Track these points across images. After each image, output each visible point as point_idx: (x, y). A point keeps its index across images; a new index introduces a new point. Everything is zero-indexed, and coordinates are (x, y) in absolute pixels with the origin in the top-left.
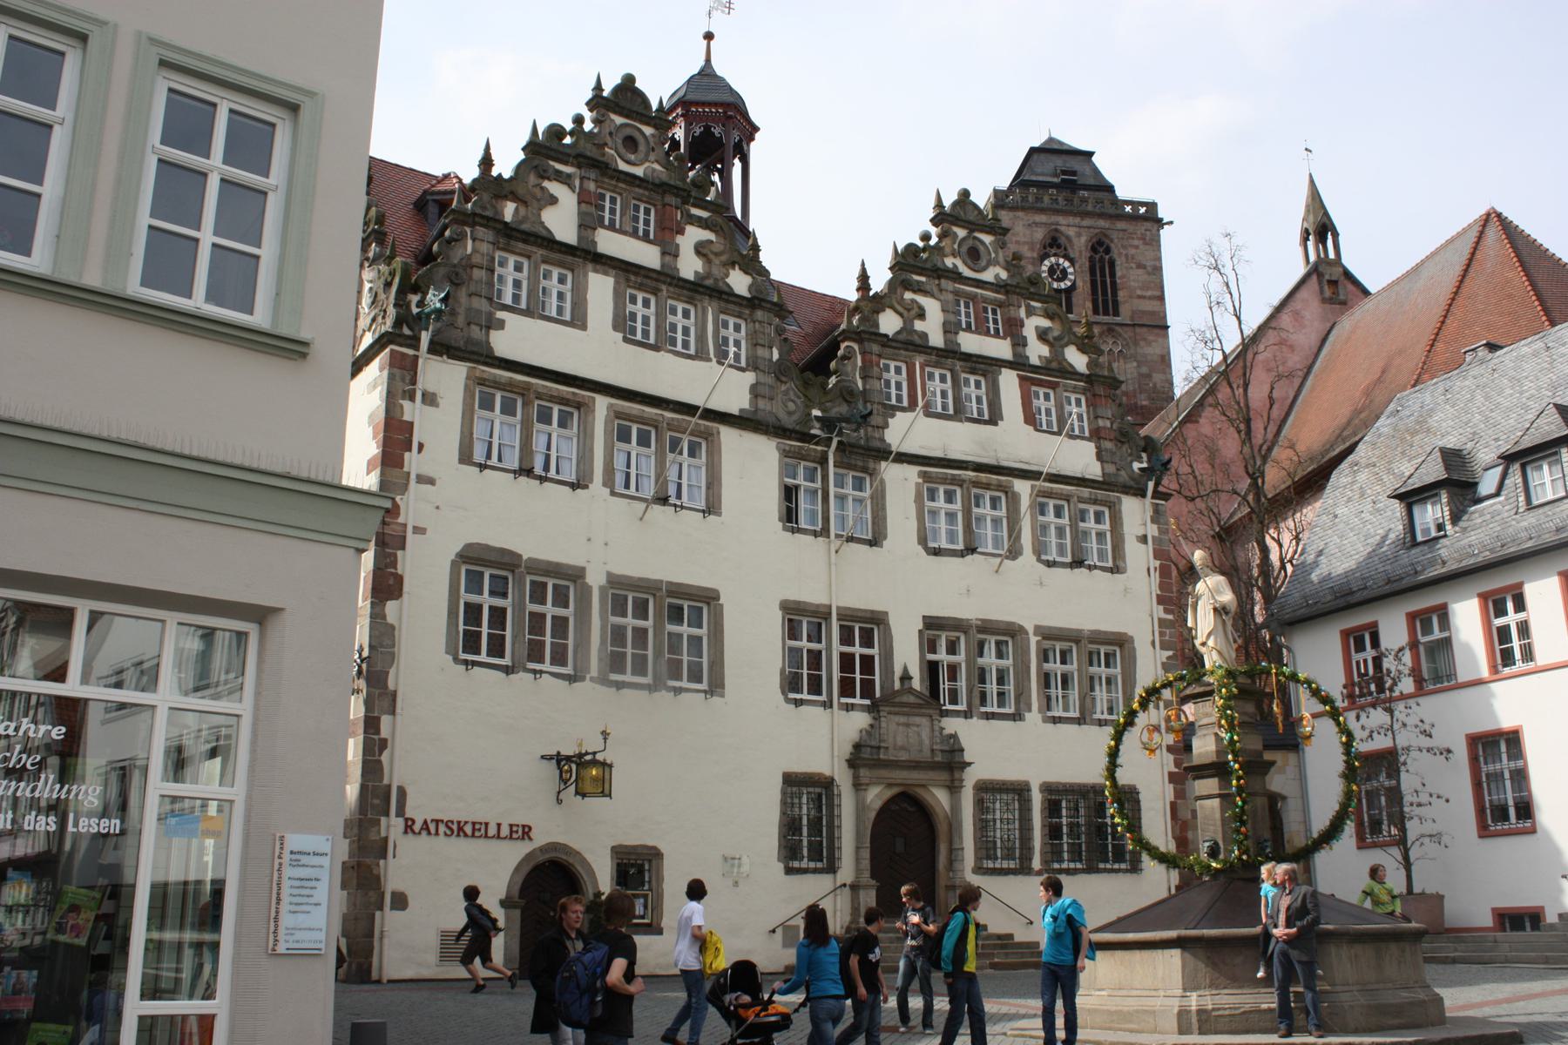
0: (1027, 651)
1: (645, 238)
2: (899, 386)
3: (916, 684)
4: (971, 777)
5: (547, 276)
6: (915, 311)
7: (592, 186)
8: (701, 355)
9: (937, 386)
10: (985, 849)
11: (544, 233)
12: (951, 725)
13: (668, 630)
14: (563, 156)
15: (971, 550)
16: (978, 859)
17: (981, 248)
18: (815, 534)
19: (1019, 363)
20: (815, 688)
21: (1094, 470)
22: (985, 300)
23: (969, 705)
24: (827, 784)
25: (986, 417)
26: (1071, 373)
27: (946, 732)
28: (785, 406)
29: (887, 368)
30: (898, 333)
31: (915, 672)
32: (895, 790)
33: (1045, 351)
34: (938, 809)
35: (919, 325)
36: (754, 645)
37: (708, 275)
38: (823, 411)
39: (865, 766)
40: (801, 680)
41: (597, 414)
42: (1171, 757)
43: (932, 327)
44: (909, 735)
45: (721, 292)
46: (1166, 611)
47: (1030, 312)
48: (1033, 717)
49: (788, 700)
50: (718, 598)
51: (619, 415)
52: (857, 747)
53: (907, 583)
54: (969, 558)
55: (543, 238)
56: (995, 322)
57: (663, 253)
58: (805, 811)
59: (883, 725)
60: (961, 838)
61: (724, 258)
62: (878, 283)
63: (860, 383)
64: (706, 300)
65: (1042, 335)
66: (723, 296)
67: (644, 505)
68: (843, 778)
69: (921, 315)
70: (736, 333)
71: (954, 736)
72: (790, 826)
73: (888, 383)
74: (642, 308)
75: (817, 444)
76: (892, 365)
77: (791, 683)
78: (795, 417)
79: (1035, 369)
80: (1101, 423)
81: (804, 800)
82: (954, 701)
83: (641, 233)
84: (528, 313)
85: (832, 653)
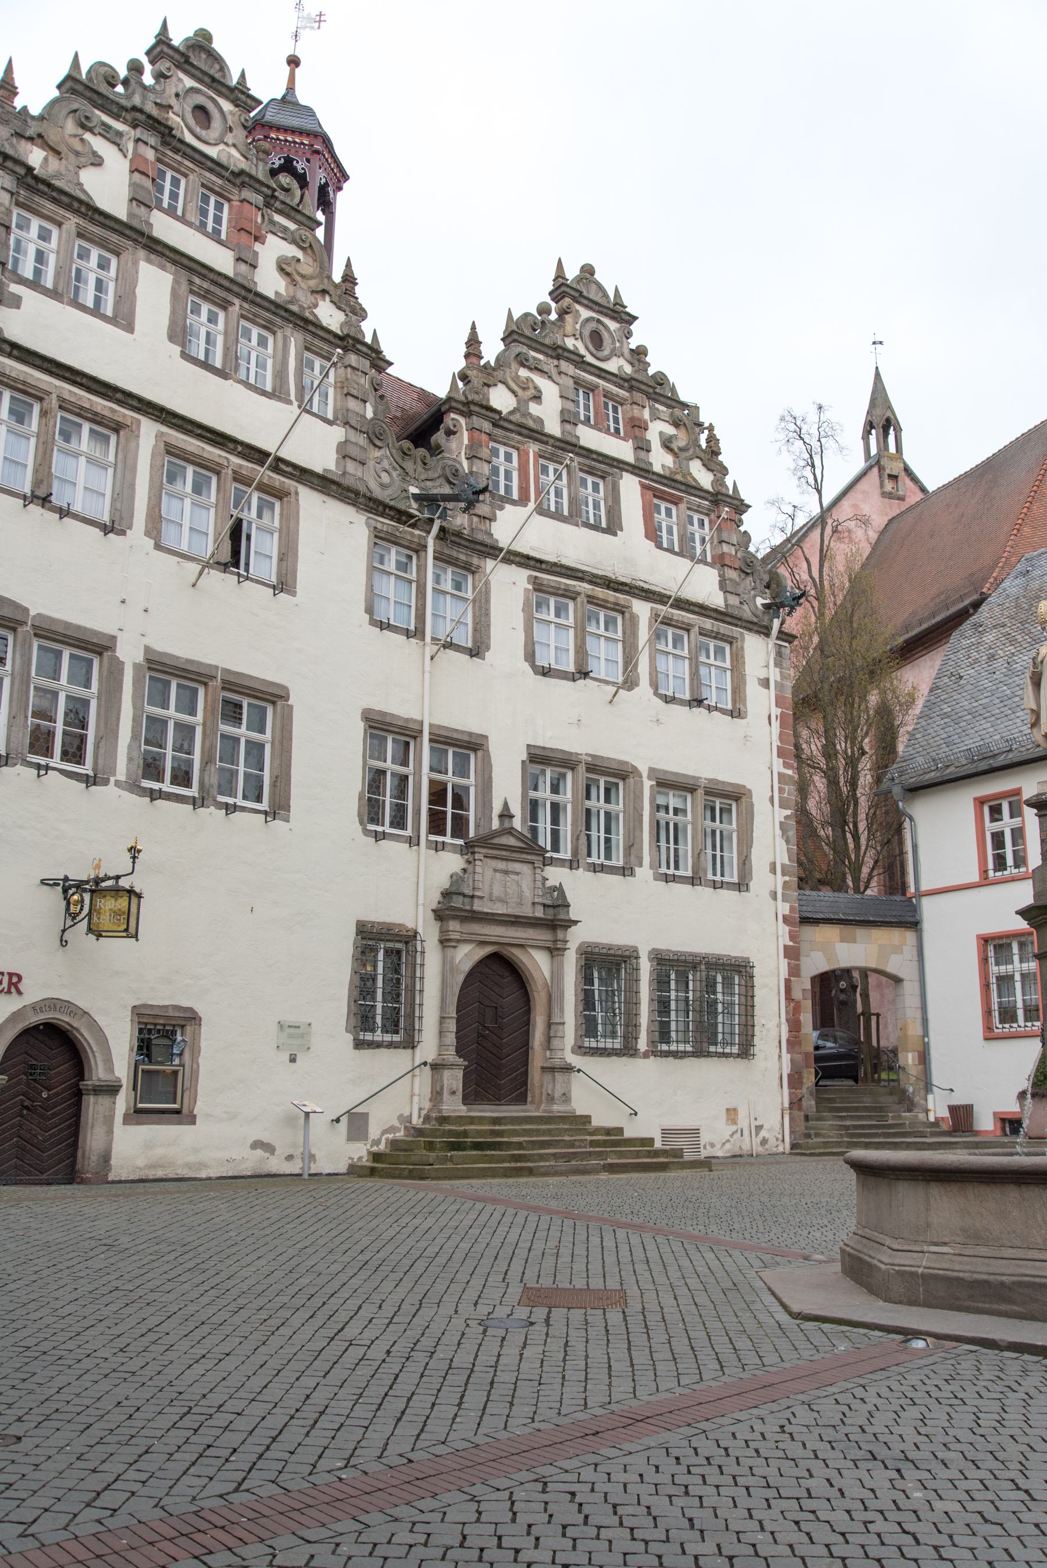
0: (638, 797)
1: (215, 236)
2: (508, 475)
3: (517, 824)
4: (576, 937)
5: (84, 255)
6: (532, 392)
7: (150, 155)
8: (278, 394)
9: (556, 481)
10: (588, 1027)
11: (83, 197)
12: (555, 875)
13: (217, 736)
14: (116, 110)
15: (583, 673)
16: (579, 1037)
17: (605, 335)
18: (408, 634)
19: (641, 470)
20: (399, 821)
21: (717, 600)
22: (607, 395)
23: (575, 852)
24: (410, 938)
25: (604, 525)
26: (695, 489)
27: (548, 884)
28: (380, 473)
29: (495, 453)
30: (511, 413)
31: (516, 809)
32: (488, 950)
33: (669, 460)
34: (536, 975)
35: (534, 408)
36: (328, 761)
37: (293, 300)
38: (421, 489)
39: (455, 917)
40: (381, 807)
41: (142, 441)
42: (787, 929)
43: (548, 411)
44: (506, 887)
45: (306, 321)
46: (786, 765)
47: (655, 416)
48: (644, 872)
49: (366, 832)
50: (286, 697)
51: (171, 450)
52: (446, 894)
53: (511, 705)
54: (581, 682)
55: (81, 202)
56: (616, 421)
57: (239, 259)
58: (380, 970)
59: (478, 869)
60: (562, 1011)
61: (312, 283)
62: (491, 349)
63: (465, 464)
64: (289, 330)
65: (667, 444)
66: (307, 324)
67: (196, 567)
68: (429, 933)
69: (537, 398)
70: (325, 377)
71: (560, 889)
72: (363, 988)
73: (495, 471)
74: (209, 325)
75: (413, 526)
76: (502, 450)
77: (371, 811)
79: (660, 478)
80: (725, 548)
81: (381, 956)
82: (556, 848)
83: (210, 229)
84: (54, 294)
85: (419, 781)
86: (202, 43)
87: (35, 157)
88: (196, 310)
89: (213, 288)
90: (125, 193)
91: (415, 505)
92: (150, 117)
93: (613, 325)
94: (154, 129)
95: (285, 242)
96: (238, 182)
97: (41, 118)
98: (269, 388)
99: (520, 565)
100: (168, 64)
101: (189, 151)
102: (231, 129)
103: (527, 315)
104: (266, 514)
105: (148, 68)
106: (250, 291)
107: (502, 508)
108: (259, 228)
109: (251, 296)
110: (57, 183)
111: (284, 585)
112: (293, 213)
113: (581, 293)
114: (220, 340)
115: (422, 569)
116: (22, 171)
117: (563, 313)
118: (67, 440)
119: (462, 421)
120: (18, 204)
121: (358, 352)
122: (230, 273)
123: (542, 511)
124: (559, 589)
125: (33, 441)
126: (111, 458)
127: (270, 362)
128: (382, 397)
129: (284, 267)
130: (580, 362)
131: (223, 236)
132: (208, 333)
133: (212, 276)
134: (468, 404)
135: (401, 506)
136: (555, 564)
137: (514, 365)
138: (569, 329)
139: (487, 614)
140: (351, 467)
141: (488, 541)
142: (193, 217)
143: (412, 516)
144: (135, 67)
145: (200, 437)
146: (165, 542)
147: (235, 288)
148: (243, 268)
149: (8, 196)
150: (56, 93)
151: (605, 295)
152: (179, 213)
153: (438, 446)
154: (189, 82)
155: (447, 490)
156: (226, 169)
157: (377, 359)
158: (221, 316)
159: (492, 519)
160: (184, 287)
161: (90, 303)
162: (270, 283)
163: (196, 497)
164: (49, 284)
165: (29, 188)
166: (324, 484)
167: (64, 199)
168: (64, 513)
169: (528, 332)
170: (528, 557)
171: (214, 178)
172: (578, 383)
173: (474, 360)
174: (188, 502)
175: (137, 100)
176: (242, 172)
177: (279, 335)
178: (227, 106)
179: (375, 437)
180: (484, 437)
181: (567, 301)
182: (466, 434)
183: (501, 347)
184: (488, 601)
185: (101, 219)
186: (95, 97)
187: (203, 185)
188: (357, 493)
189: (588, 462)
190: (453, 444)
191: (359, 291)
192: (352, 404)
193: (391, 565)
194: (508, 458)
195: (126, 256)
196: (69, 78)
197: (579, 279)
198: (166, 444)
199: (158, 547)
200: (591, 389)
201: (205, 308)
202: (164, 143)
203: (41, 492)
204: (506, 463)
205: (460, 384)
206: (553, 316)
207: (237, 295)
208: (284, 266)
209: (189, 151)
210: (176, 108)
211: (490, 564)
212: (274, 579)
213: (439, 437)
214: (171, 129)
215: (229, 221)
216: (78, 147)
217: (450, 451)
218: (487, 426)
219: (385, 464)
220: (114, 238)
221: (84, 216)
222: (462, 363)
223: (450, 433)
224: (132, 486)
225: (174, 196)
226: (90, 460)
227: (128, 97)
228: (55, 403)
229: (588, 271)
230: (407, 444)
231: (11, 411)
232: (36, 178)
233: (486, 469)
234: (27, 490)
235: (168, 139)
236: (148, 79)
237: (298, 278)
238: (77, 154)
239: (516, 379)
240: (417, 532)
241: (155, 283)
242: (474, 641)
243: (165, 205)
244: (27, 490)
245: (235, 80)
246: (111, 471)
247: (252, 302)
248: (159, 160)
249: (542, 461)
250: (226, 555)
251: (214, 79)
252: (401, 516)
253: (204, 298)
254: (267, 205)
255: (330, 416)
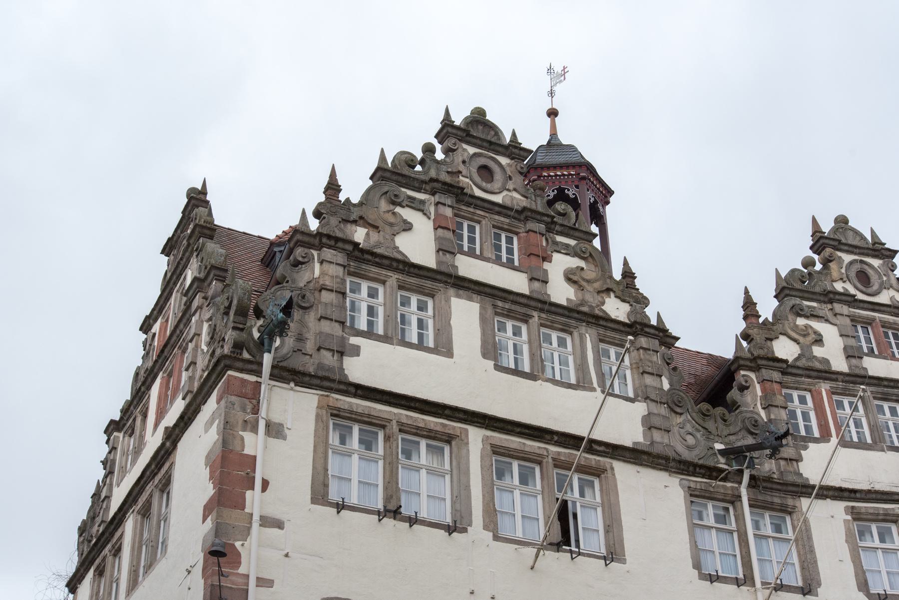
1: (510, 265)
5: (405, 302)
6: (812, 337)
7: (449, 212)
8: (583, 384)
9: (852, 412)
11: (400, 257)
17: (870, 272)
18: (737, 582)
22: (885, 325)
29: (789, 398)
30: (797, 359)
35: (817, 351)
37: (583, 303)
38: (725, 444)
43: (832, 350)
45: (597, 318)
51: (497, 450)
55: (398, 261)
57: (532, 279)
61: (597, 285)
62: (767, 308)
63: (763, 413)
64: (583, 329)
66: (599, 320)
67: (531, 551)
69: (819, 341)
70: (620, 361)
73: (793, 414)
74: (514, 338)
75: (725, 479)
76: (795, 394)
78: (696, 452)
83: (504, 260)
84: (385, 339)
86: (478, 118)
87: (359, 235)
88: (502, 328)
89: (514, 307)
90: (432, 247)
91: (722, 460)
92: (445, 183)
93: (876, 263)
94: (449, 192)
95: (568, 257)
96: (522, 217)
97: (361, 204)
98: (573, 381)
99: (834, 498)
100: (454, 141)
101: (479, 203)
102: (510, 178)
103: (793, 271)
104: (588, 492)
105: (438, 147)
106: (545, 303)
107: (806, 448)
108: (545, 250)
109: (546, 307)
110: (378, 251)
111: (613, 554)
112: (572, 232)
113: (839, 241)
114: (526, 348)
115: (740, 518)
116: (350, 248)
117: (826, 263)
118: (409, 457)
119: (752, 375)
120: (350, 274)
121: (647, 335)
122: (526, 292)
123: (845, 443)
124: (878, 514)
125: (381, 463)
126: (447, 466)
127: (571, 359)
128: (675, 369)
129: (570, 277)
130: (852, 301)
131: (516, 263)
132: (515, 345)
133: (511, 297)
134: (755, 359)
135: (710, 463)
136: (869, 491)
137: (791, 317)
138: (835, 274)
139: (812, 550)
140: (657, 436)
141: (799, 481)
142: (489, 254)
143: (722, 471)
144: (429, 149)
145: (521, 434)
146: (502, 533)
147: (533, 303)
148: (536, 285)
149: (341, 269)
150: (370, 183)
151: (863, 238)
152: (478, 252)
153: (734, 403)
154: (472, 150)
155: (750, 441)
156: (511, 209)
157: (664, 337)
158: (524, 328)
159: (799, 459)
160: (490, 311)
161: (415, 340)
162: (561, 292)
163: (524, 488)
164: (381, 331)
165: (357, 259)
166: (634, 455)
167: (386, 262)
168: (413, 521)
169: (798, 285)
170: (841, 489)
171: (502, 219)
172: (854, 320)
173: (753, 320)
174: (517, 493)
175: (433, 174)
176: (525, 209)
177: (576, 334)
178: (504, 161)
179: (674, 404)
180: (776, 387)
181: (828, 251)
182: (758, 387)
183: (776, 303)
184: (810, 538)
185: (416, 271)
186: (400, 179)
187: (494, 226)
188: (667, 459)
189: (880, 389)
190: (748, 397)
191: (638, 283)
192: (649, 380)
193: (710, 520)
194: (803, 400)
195: (439, 296)
196: (378, 169)
197: (835, 230)
198: (492, 446)
199: (496, 538)
200: (867, 323)
201: (509, 325)
202: (458, 201)
203: (392, 507)
204: (801, 406)
205: (744, 344)
206: (818, 267)
207: (535, 308)
208: (571, 276)
209: (479, 203)
210: (464, 172)
211: (805, 502)
212: (603, 551)
213: (734, 394)
214: (463, 189)
215: (520, 250)
216: (391, 219)
217: (747, 405)
218: (776, 376)
219: (689, 427)
220: (428, 284)
221: (402, 272)
222: (742, 325)
223: (743, 388)
224: (468, 487)
225: (472, 240)
226: (430, 471)
227: (425, 172)
228: (395, 428)
229: (842, 221)
230: (705, 406)
231: (361, 441)
232: (362, 251)
233: (783, 414)
234: (380, 506)
235: (461, 197)
236: (439, 155)
237: (584, 284)
238: (391, 225)
239: (795, 328)
240: (729, 485)
241: (465, 314)
242: (804, 579)
243: (466, 249)
244: (380, 506)
245: (508, 138)
246: (448, 477)
247: (549, 312)
248: (456, 215)
249: (835, 397)
250: (557, 536)
251: (491, 143)
252: (712, 472)
253: (508, 316)
254: (549, 230)
255: (631, 394)
